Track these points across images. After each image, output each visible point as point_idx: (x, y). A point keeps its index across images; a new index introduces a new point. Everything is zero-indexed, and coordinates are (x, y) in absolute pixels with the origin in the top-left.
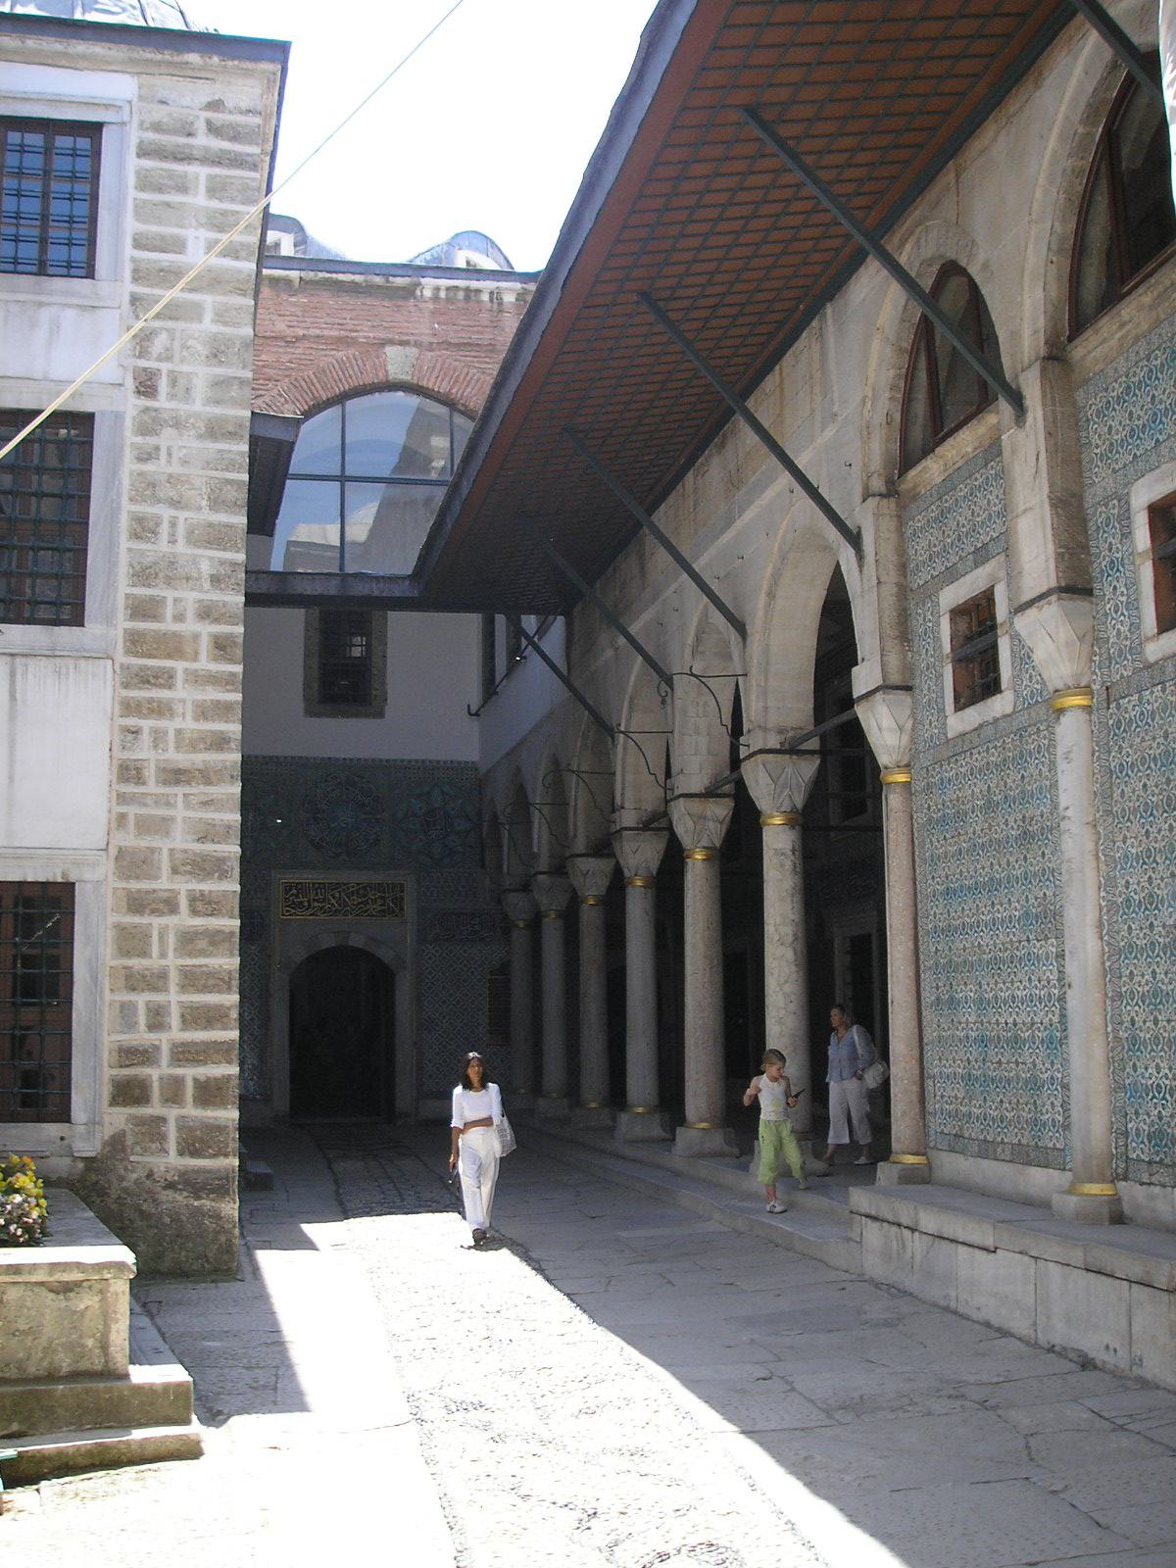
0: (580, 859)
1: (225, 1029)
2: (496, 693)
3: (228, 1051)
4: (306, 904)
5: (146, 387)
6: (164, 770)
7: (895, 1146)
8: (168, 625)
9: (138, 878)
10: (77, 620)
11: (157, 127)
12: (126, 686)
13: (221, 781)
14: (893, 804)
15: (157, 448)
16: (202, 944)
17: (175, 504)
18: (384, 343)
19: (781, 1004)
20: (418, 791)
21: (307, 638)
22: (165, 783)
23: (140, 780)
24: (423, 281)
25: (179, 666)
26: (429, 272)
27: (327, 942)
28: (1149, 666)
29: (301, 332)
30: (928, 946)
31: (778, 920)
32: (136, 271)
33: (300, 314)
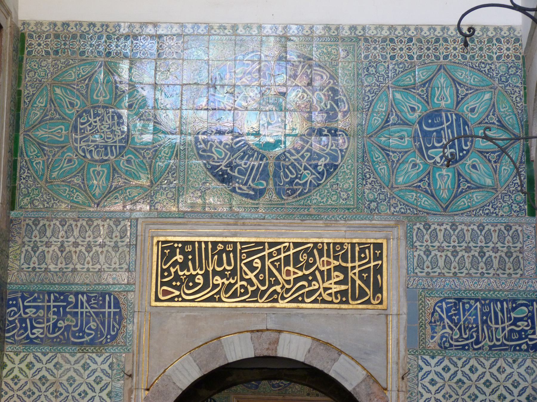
4: (200, 280)
20: (408, 80)
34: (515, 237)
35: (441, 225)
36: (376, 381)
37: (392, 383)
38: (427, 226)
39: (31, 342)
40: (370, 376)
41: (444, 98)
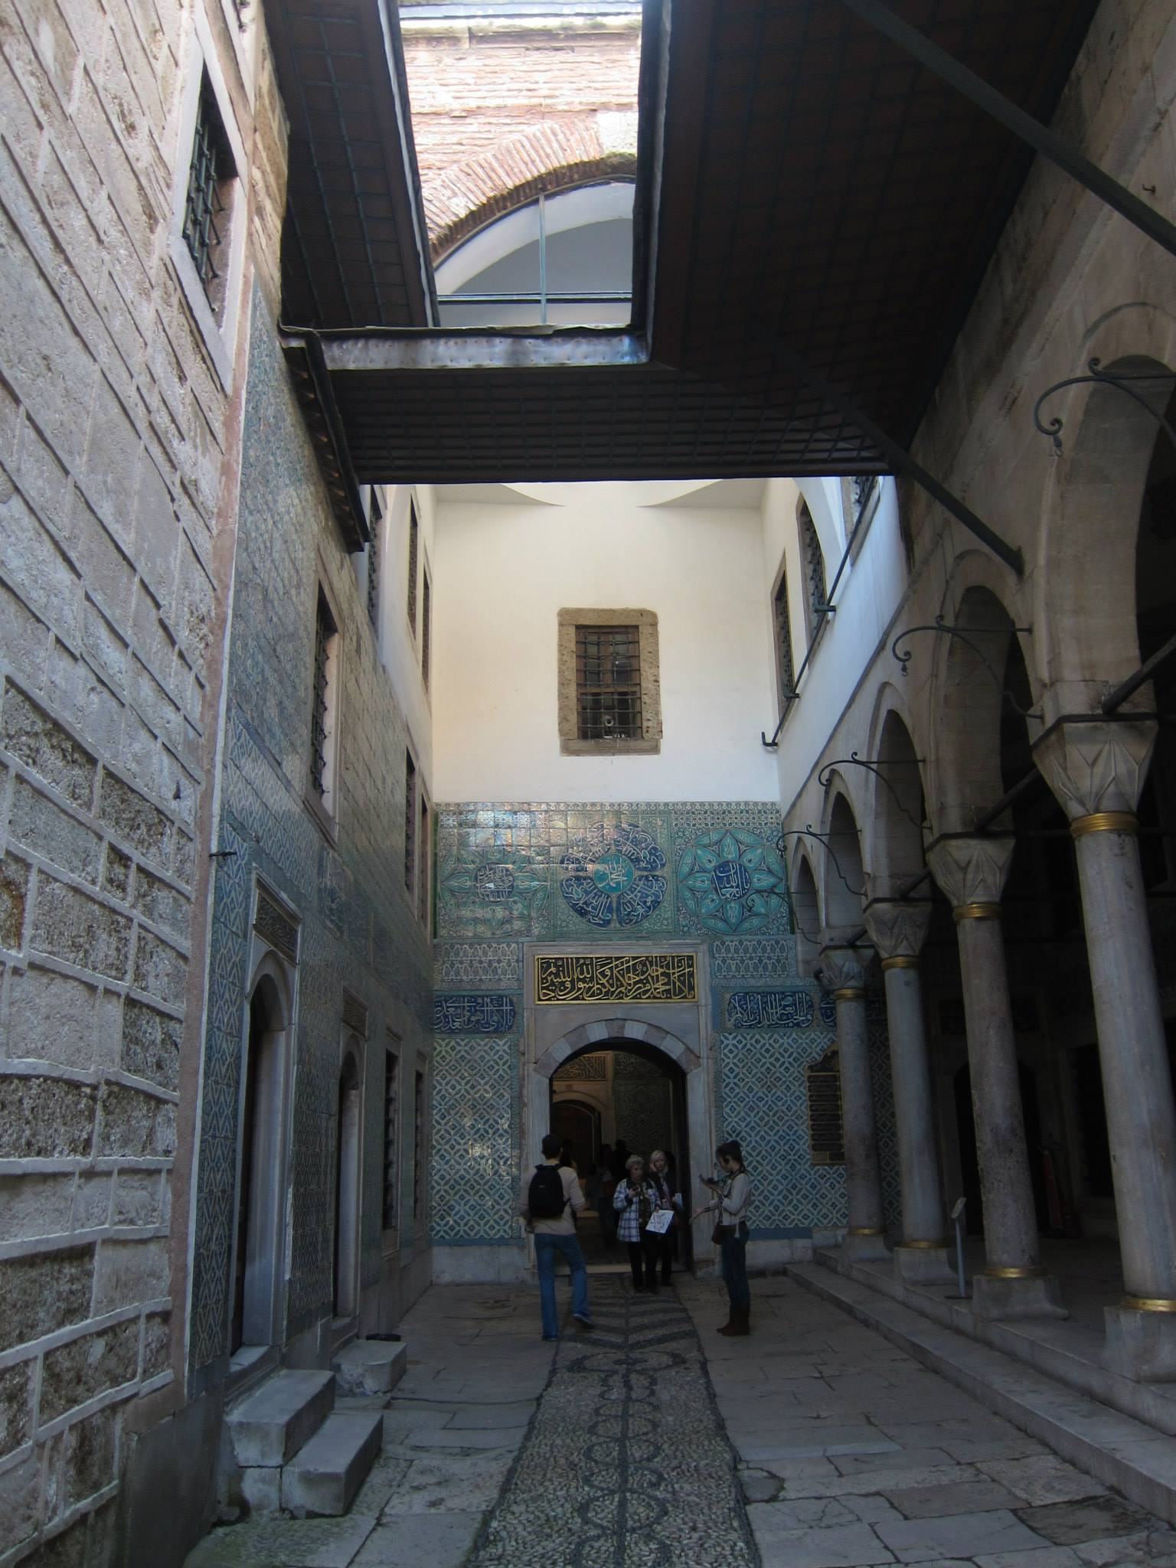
0: (954, 842)
2: (797, 696)
20: (706, 841)
21: (562, 662)
29: (472, 104)
33: (471, 81)
34: (782, 949)
35: (732, 942)
36: (692, 1052)
37: (704, 1053)
38: (723, 943)
39: (452, 1031)
40: (688, 1049)
41: (730, 853)
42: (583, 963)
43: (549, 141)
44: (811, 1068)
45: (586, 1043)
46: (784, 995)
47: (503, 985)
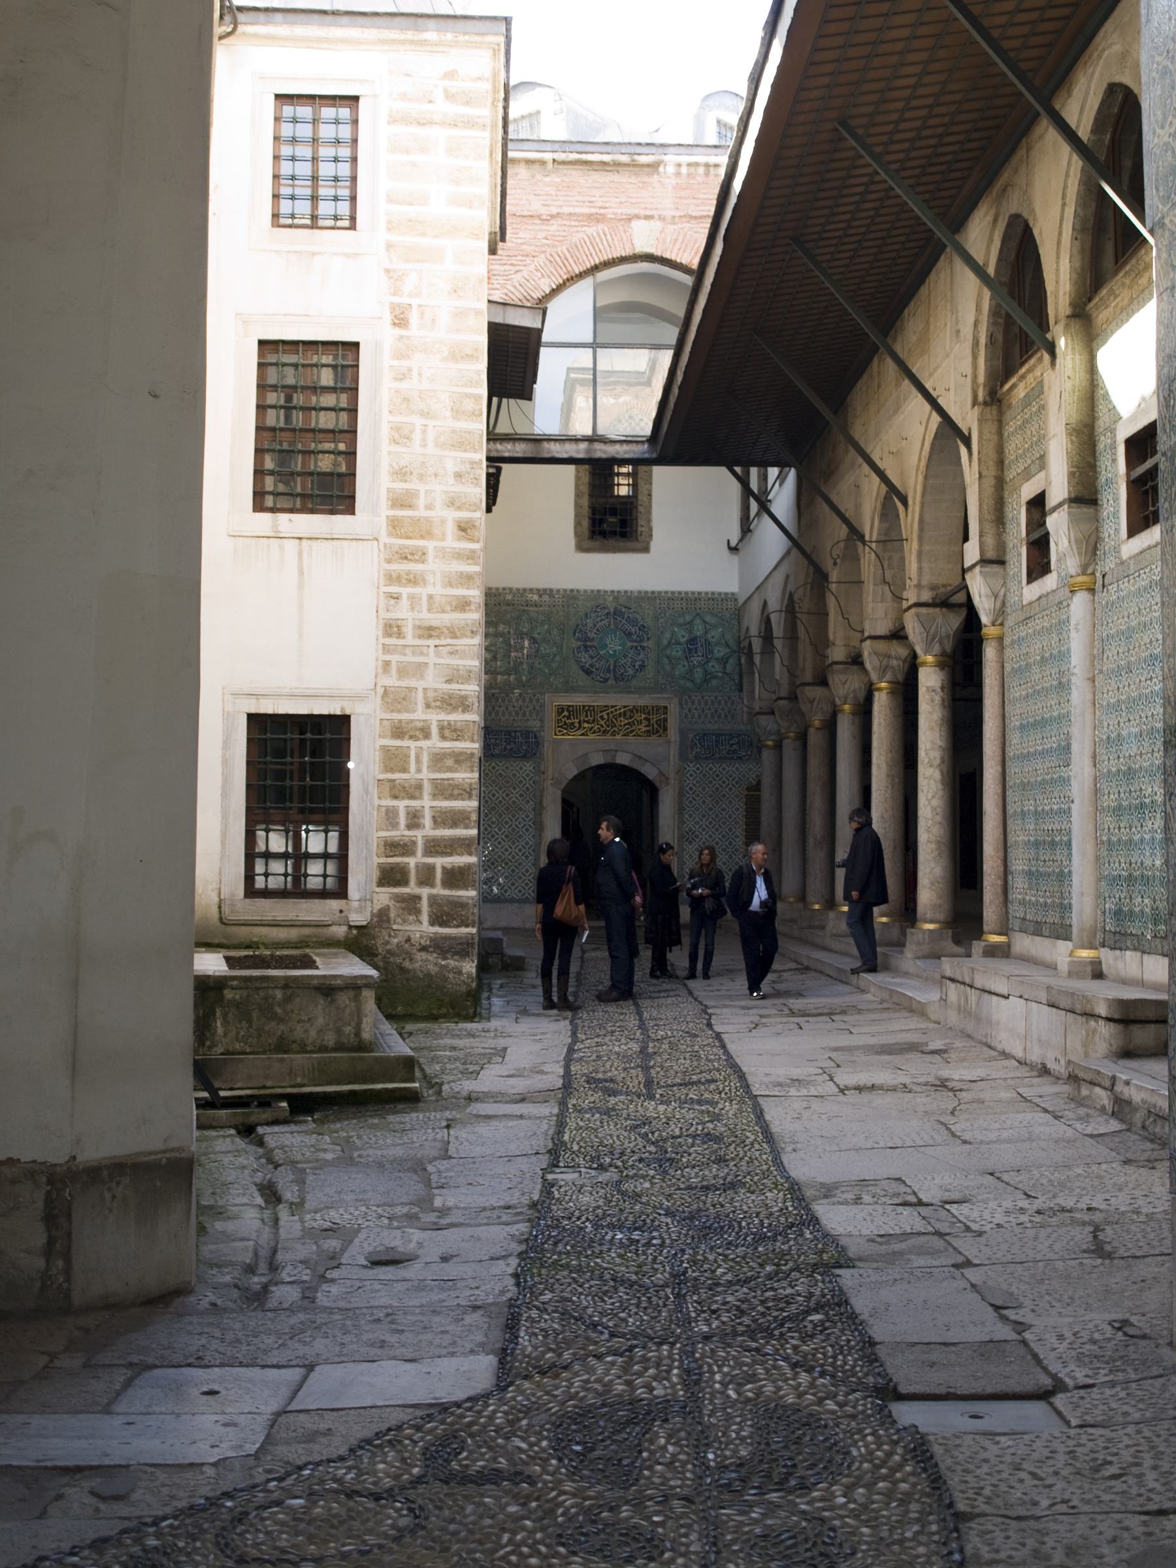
1: (467, 827)
2: (750, 531)
3: (469, 846)
4: (577, 725)
5: (400, 321)
6: (419, 627)
7: (985, 928)
8: (421, 512)
9: (399, 711)
10: (350, 510)
11: (404, 96)
12: (389, 561)
13: (464, 636)
14: (989, 653)
15: (410, 370)
16: (450, 762)
17: (425, 414)
18: (629, 219)
19: (930, 816)
20: (681, 621)
22: (420, 637)
23: (400, 635)
24: (666, 158)
25: (430, 545)
26: (671, 149)
27: (597, 760)
28: (1122, 563)
29: (554, 211)
30: (1013, 769)
31: (929, 745)
32: (389, 222)
33: (553, 193)
34: (733, 703)
37: (672, 775)
41: (699, 630)
42: (589, 710)
43: (601, 240)
44: (748, 789)
45: (588, 766)
46: (731, 736)
47: (530, 723)
